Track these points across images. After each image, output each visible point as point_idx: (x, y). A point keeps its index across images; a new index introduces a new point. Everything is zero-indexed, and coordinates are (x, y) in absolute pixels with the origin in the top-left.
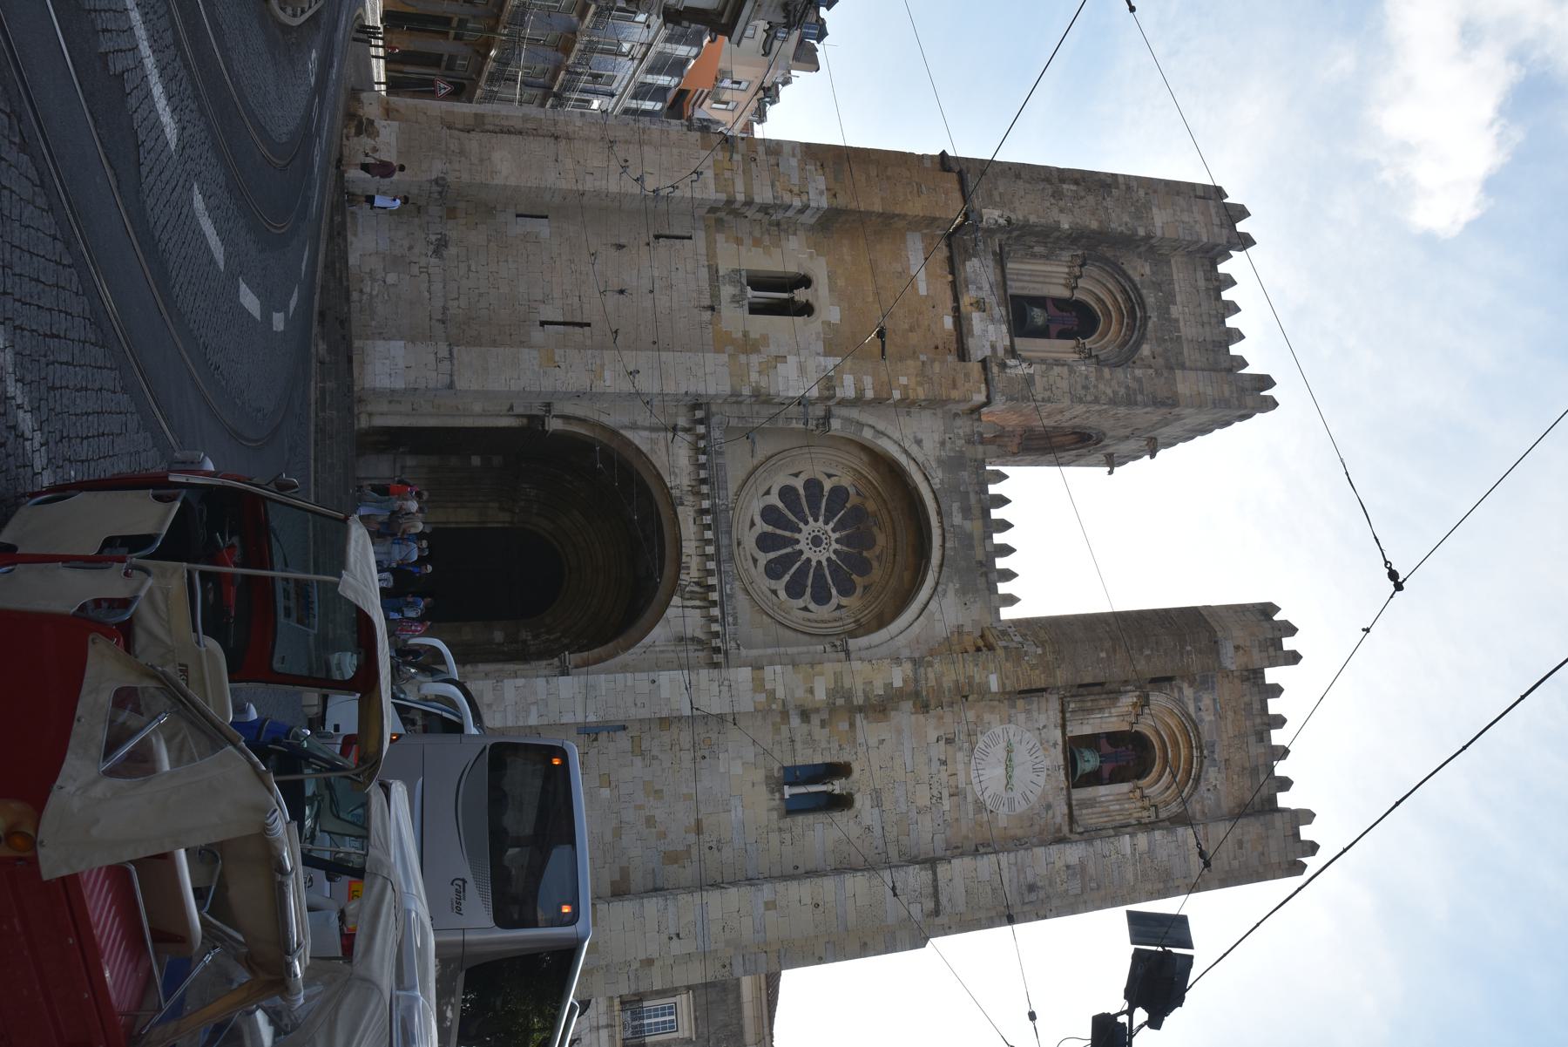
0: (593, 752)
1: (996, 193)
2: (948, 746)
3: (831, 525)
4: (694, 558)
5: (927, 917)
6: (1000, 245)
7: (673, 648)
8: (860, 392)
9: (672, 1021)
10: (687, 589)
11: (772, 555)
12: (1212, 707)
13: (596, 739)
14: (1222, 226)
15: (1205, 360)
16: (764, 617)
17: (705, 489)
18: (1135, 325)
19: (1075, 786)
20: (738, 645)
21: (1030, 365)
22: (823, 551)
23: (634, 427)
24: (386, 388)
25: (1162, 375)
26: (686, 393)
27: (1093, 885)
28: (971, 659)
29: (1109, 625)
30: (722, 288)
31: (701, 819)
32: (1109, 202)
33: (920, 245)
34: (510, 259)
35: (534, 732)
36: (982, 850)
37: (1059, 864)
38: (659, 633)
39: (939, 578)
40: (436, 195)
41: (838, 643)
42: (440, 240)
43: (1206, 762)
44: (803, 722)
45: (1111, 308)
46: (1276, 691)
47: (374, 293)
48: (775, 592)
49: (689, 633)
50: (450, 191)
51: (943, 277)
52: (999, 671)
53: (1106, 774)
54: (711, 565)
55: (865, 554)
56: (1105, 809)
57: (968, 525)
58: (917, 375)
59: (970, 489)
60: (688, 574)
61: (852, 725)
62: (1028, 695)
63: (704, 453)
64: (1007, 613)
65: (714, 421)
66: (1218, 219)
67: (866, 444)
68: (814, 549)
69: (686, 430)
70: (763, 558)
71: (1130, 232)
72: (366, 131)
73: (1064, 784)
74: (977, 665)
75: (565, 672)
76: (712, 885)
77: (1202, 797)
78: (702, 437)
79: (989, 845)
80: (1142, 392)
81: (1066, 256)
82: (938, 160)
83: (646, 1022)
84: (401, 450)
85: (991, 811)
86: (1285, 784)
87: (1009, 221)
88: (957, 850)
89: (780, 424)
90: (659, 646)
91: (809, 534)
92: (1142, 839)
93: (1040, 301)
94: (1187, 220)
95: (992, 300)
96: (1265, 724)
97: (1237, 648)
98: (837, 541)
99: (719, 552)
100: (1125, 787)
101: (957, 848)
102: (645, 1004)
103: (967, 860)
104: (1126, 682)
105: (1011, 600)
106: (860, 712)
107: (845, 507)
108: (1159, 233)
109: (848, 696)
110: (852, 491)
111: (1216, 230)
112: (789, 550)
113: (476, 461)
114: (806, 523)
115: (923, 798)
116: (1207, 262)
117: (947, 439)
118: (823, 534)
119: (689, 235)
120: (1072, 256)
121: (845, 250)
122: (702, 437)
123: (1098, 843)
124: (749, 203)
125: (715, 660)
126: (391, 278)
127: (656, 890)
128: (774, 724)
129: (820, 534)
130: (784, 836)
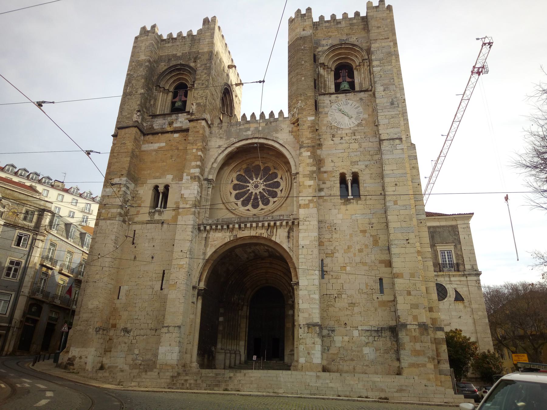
0: (332, 273)
1: (128, 116)
2: (336, 136)
3: (251, 181)
4: (257, 231)
5: (402, 142)
6: (150, 116)
8: (198, 166)
9: (447, 253)
10: (269, 234)
11: (260, 203)
12: (326, 40)
13: (327, 271)
14: (147, 35)
15: (198, 44)
16: (283, 206)
17: (231, 226)
18: (183, 68)
20: (292, 214)
21: (192, 104)
23: (204, 254)
24: (178, 355)
25: (200, 57)
26: (192, 232)
27: (392, 81)
28: (301, 127)
29: (292, 77)
30: (155, 219)
31: (360, 231)
32: (135, 75)
33: (147, 145)
34: (135, 302)
35: (322, 297)
36: (377, 124)
37: (383, 93)
38: (285, 246)
39: (271, 140)
40: (105, 332)
41: (293, 177)
42: (123, 330)
43: (347, 42)
44: (323, 191)
45: (177, 78)
46: (322, 18)
47: (141, 359)
48: (274, 202)
49: (286, 234)
50: (103, 326)
51: (159, 136)
52: (306, 117)
53: (350, 80)
54: (260, 224)
55: (262, 169)
56: (363, 79)
57: (252, 129)
58: (193, 146)
59: (238, 128)
60: (263, 233)
61: (325, 172)
62: (318, 107)
63: (217, 226)
64: (286, 115)
65: (205, 222)
66: (145, 37)
67: (220, 167)
70: (261, 206)
71: (147, 68)
72: (72, 361)
73: (353, 94)
74: (304, 125)
75: (297, 284)
77: (361, 43)
78: (211, 227)
79: (375, 121)
80: (206, 64)
81: (155, 92)
82: (115, 138)
83: (447, 262)
84: (213, 349)
85: (362, 120)
86: (357, 14)
87: (139, 111)
88: (377, 134)
89: (209, 198)
92: (375, 63)
93: (173, 103)
94: (144, 48)
95: (169, 119)
96: (334, 21)
97: (304, 30)
98: (257, 179)
100: (356, 73)
101: (375, 133)
102: (440, 262)
103: (380, 128)
104: (315, 71)
105: (281, 113)
106: (319, 169)
107: (244, 176)
108: (148, 58)
109: (314, 172)
110: (238, 173)
111: (149, 37)
112: (259, 197)
113: (221, 319)
114: (249, 190)
115: (355, 146)
116: (162, 43)
117: (219, 136)
119: (134, 231)
120: (156, 90)
121: (146, 173)
122: (211, 227)
123: (376, 79)
124: (121, 207)
125: (297, 223)
126: (136, 352)
127: (389, 249)
128: (323, 202)
130: (368, 198)
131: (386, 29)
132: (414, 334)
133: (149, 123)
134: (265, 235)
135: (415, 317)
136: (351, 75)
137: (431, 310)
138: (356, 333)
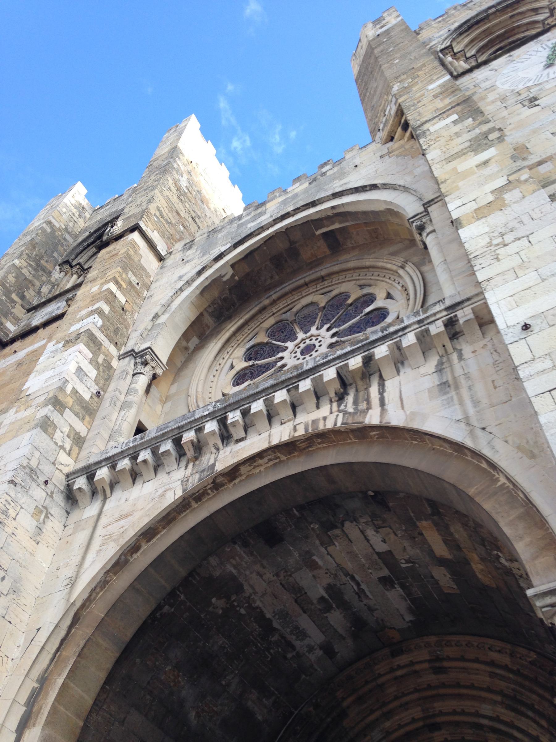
4: (298, 421)
6: (29, 311)
7: (465, 392)
22: (320, 338)
60: (325, 419)
68: (317, 344)
69: (105, 498)
90: (465, 412)
91: (298, 359)
95: (70, 295)
99: (283, 382)
107: (267, 343)
110: (251, 343)
118: (299, 347)
122: (113, 467)
129: (299, 351)
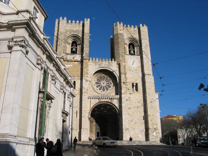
11: (105, 90)
17: (99, 98)
19: (135, 54)
23: (90, 106)
54: (108, 98)
57: (104, 64)
70: (106, 90)
76: (145, 101)
78: (92, 98)
87: (64, 53)
92: (143, 47)
97: (120, 31)
100: (135, 48)
108: (64, 31)
115: (136, 74)
127: (146, 108)
131: (146, 36)
132: (153, 131)
133: (65, 57)
134: (110, 101)
135: (153, 127)
136: (134, 48)
137: (156, 125)
138: (137, 131)
